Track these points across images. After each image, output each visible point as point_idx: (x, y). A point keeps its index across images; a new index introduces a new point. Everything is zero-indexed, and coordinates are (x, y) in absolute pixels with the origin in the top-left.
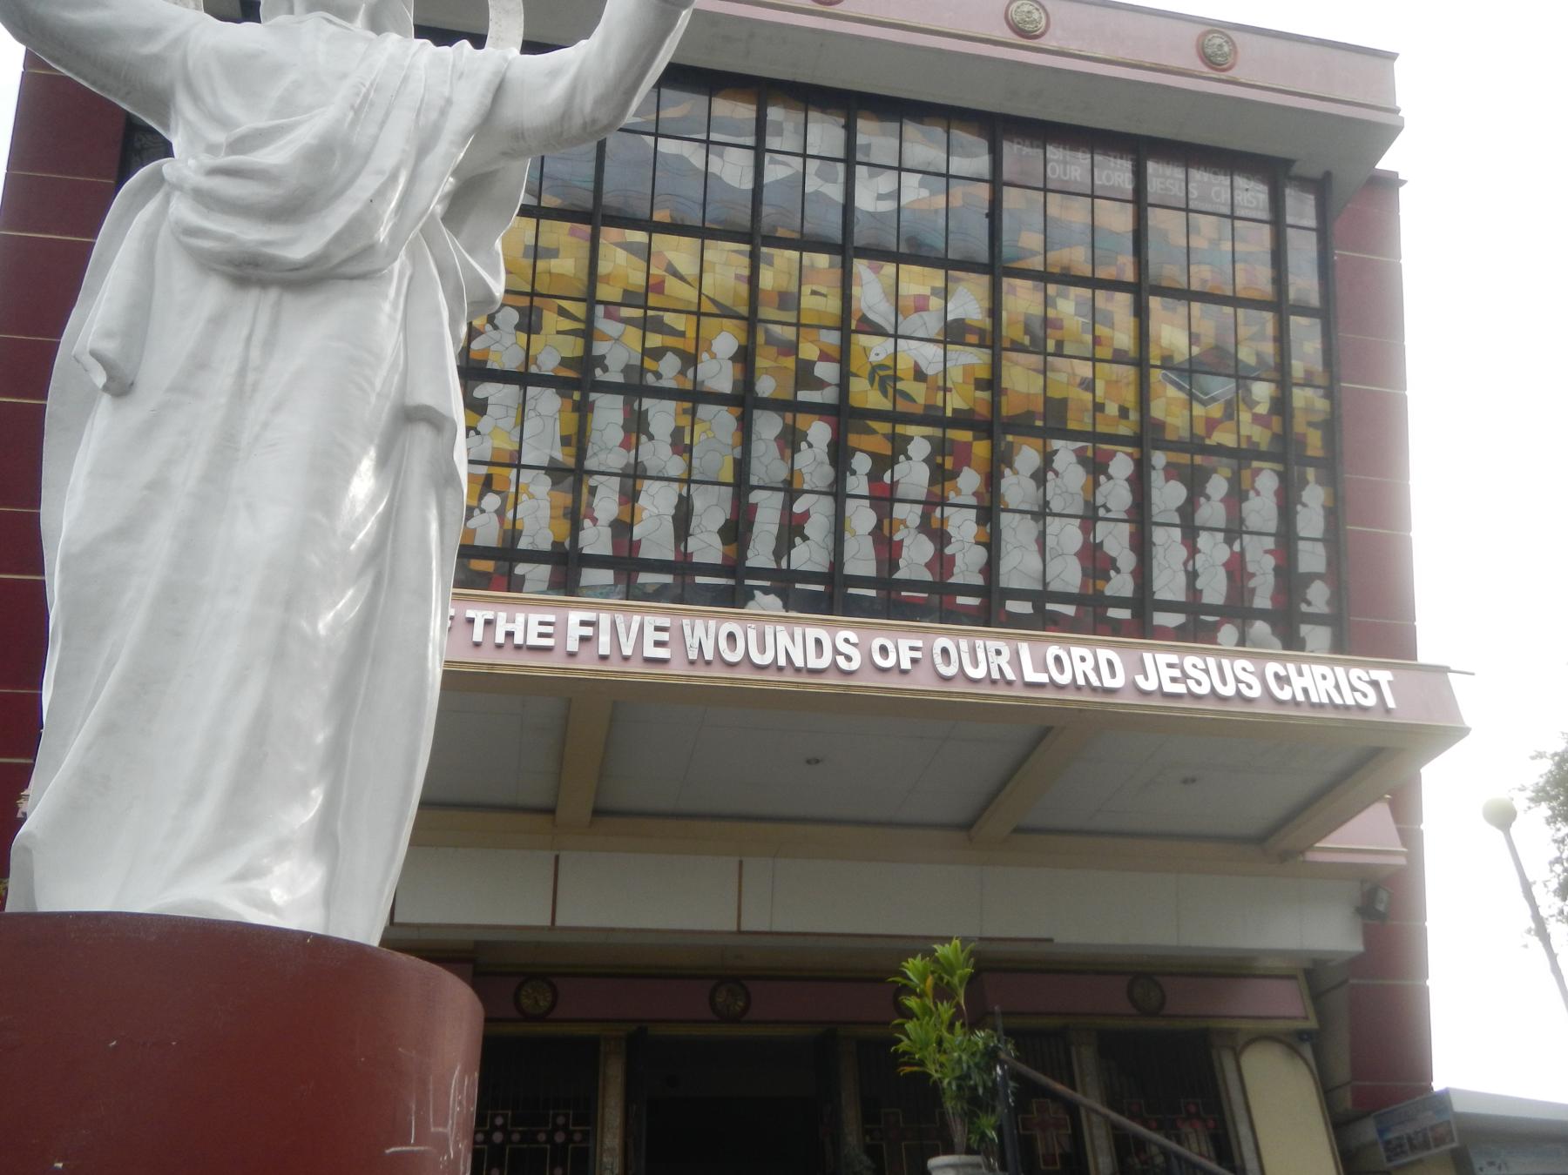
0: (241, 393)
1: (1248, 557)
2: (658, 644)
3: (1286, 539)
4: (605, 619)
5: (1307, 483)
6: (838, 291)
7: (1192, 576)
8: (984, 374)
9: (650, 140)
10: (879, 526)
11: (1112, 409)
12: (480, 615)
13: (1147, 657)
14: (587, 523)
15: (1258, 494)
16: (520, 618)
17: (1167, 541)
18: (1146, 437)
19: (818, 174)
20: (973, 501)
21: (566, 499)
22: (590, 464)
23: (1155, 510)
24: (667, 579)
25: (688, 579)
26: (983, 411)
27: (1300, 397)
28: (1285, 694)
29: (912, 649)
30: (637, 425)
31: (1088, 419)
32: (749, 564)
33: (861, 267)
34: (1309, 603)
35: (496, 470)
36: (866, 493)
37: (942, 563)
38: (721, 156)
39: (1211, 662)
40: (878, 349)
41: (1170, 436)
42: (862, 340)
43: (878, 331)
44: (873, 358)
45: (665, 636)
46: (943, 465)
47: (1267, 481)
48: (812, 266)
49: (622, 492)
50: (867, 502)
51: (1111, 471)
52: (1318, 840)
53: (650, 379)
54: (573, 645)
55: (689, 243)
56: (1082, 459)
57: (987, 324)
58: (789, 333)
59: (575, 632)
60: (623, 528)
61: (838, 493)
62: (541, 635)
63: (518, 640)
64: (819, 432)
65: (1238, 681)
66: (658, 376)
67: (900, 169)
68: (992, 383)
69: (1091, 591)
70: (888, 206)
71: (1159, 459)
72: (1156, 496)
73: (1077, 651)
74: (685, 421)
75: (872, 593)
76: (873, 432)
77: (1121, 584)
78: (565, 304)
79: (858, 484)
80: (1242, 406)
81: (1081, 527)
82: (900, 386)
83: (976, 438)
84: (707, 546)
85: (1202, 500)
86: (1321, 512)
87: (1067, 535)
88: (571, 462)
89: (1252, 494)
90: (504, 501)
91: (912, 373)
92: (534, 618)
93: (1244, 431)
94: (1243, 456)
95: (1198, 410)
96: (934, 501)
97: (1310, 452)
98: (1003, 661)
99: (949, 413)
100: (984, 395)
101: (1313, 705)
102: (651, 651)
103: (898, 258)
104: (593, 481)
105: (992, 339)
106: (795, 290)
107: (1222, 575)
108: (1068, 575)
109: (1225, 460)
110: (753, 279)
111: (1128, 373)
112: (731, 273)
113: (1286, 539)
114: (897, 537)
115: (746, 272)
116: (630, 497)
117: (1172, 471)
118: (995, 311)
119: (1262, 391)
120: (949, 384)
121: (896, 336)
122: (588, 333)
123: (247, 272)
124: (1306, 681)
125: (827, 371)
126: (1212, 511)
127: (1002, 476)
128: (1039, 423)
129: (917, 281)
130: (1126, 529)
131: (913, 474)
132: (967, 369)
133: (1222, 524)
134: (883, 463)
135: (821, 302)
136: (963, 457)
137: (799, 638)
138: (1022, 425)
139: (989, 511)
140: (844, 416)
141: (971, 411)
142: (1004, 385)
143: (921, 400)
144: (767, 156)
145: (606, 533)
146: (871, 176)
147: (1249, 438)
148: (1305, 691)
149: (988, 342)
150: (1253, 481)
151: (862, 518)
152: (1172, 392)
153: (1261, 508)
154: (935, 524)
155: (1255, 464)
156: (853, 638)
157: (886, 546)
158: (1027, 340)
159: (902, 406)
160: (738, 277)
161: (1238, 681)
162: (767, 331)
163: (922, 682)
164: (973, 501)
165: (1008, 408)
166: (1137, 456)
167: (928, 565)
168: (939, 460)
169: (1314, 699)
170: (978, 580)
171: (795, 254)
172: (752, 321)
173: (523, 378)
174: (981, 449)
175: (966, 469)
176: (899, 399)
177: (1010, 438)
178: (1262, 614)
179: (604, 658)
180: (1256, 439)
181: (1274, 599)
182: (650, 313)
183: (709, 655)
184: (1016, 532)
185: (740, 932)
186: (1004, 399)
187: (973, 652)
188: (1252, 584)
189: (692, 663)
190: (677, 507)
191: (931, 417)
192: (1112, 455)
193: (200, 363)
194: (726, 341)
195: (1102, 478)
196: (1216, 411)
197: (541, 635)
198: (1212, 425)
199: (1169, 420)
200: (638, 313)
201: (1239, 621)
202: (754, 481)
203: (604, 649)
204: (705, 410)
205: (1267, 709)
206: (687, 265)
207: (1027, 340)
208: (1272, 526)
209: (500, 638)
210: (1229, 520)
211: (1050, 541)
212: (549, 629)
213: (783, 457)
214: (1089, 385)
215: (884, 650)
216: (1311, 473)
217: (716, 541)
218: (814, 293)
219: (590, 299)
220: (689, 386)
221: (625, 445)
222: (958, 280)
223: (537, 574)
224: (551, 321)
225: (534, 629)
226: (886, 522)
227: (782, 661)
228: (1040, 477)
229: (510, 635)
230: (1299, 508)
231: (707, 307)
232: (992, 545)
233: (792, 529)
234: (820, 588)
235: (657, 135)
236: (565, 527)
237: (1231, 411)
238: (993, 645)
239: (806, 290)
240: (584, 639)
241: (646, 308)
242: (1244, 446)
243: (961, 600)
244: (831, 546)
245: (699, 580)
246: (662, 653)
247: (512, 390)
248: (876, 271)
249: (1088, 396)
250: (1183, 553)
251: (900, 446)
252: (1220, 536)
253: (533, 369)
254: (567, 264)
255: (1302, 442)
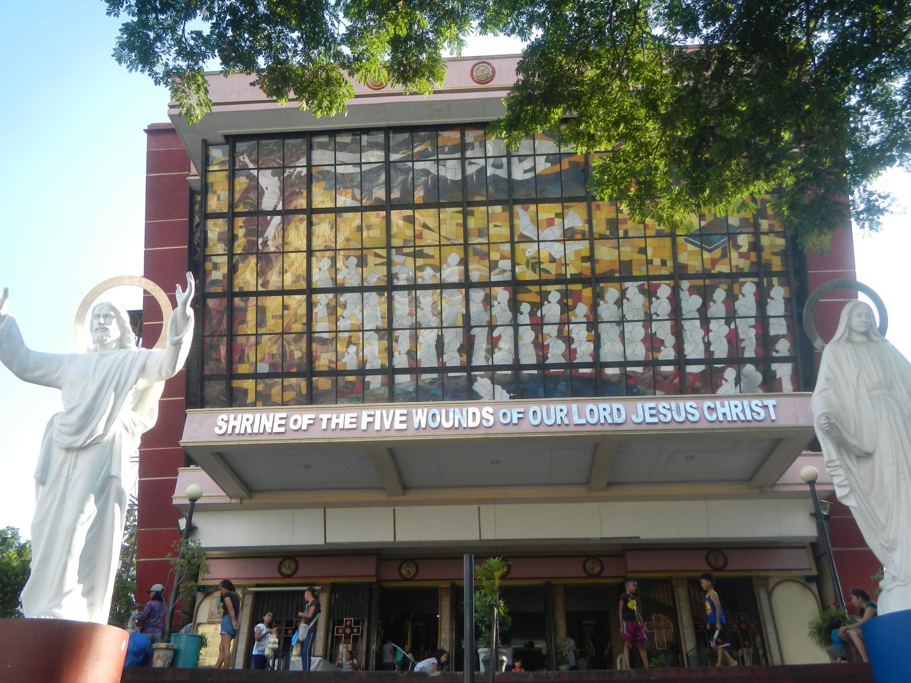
0: (67, 482)
1: (740, 331)
2: (401, 422)
3: (762, 320)
4: (378, 413)
5: (773, 286)
6: (508, 224)
7: (707, 345)
8: (586, 253)
9: (410, 164)
10: (537, 337)
11: (657, 262)
12: (325, 417)
13: (639, 405)
14: (396, 354)
15: (744, 296)
16: (342, 416)
17: (693, 330)
18: (679, 273)
19: (494, 166)
20: (585, 320)
21: (385, 343)
22: (395, 325)
23: (684, 312)
24: (435, 376)
25: (445, 375)
26: (588, 273)
27: (765, 240)
28: (714, 418)
29: (518, 413)
30: (416, 303)
31: (644, 269)
32: (473, 364)
33: (518, 209)
34: (777, 352)
35: (352, 334)
36: (529, 322)
37: (571, 353)
38: (444, 166)
39: (673, 405)
40: (530, 250)
41: (691, 271)
42: (520, 247)
43: (529, 240)
44: (527, 254)
45: (404, 418)
46: (566, 304)
47: (749, 288)
48: (494, 213)
49: (411, 338)
50: (529, 327)
51: (658, 295)
52: (778, 479)
53: (420, 281)
54: (364, 427)
55: (433, 211)
56: (641, 290)
57: (586, 228)
58: (485, 248)
59: (365, 419)
60: (412, 354)
61: (515, 325)
62: (351, 423)
63: (341, 426)
64: (502, 295)
65: (687, 412)
66: (424, 280)
67: (535, 155)
68: (590, 258)
69: (651, 359)
70: (530, 175)
71: (685, 284)
72: (684, 304)
73: (602, 406)
74: (437, 298)
75: (535, 372)
76: (530, 291)
77: (667, 353)
78: (378, 251)
79: (524, 319)
80: (732, 249)
81: (644, 326)
82: (542, 266)
83: (583, 288)
84: (453, 358)
85: (711, 303)
86: (783, 301)
87: (636, 331)
88: (386, 326)
89: (740, 296)
90: (358, 349)
91: (548, 259)
92: (348, 415)
93: (734, 263)
94: (735, 276)
95: (706, 255)
96: (564, 322)
97: (774, 269)
98: (563, 414)
99: (569, 277)
100: (588, 264)
101: (729, 422)
102: (398, 426)
103: (537, 201)
104: (397, 333)
105: (590, 237)
106: (485, 225)
107: (725, 341)
108: (638, 351)
109: (723, 280)
110: (465, 224)
111: (668, 241)
112: (454, 222)
113: (762, 320)
114: (545, 343)
115: (461, 221)
116: (415, 339)
117: (692, 290)
118: (589, 221)
119: (744, 240)
120: (568, 262)
121: (539, 241)
122: (389, 264)
123: (68, 449)
124: (726, 410)
125: (506, 264)
126: (717, 308)
127: (598, 305)
128: (617, 275)
129: (547, 211)
130: (668, 324)
131: (552, 310)
132: (577, 252)
133: (723, 314)
134: (536, 306)
135: (500, 231)
136: (578, 297)
137: (465, 412)
138: (608, 278)
139: (593, 323)
140: (515, 285)
141: (580, 273)
142: (597, 256)
143: (553, 272)
144: (467, 162)
145: (405, 357)
146: (520, 161)
147: (737, 266)
148: (724, 414)
149: (587, 237)
150: (741, 289)
151: (527, 335)
152: (690, 247)
153: (747, 303)
154: (565, 334)
155: (741, 280)
156: (491, 410)
157: (540, 347)
158: (608, 233)
159: (545, 276)
160: (457, 225)
161: (687, 412)
162: (474, 250)
163: (525, 429)
164: (585, 320)
165: (600, 269)
166: (672, 284)
167: (563, 355)
168: (565, 301)
169: (729, 418)
170: (590, 360)
171: (484, 208)
172: (466, 245)
173: (361, 289)
174: (587, 292)
175: (579, 304)
176: (542, 273)
177: (602, 285)
178: (750, 361)
179: (378, 431)
180: (741, 266)
181: (756, 351)
182: (417, 249)
183: (423, 425)
184: (609, 333)
185: (481, 540)
186: (597, 266)
187: (548, 411)
188: (743, 345)
189: (417, 429)
190: (437, 341)
191: (560, 280)
192: (659, 285)
193: (59, 475)
194: (454, 257)
195: (654, 299)
196: (718, 253)
197: (351, 423)
198: (714, 262)
199: (690, 263)
200: (412, 250)
201: (736, 366)
202: (473, 324)
203: (377, 426)
204: (447, 293)
205: (703, 425)
206: (432, 223)
207: (608, 233)
208: (753, 313)
209: (333, 427)
210: (727, 312)
211: (627, 335)
212: (354, 420)
213: (486, 310)
214: (643, 251)
215: (505, 414)
216: (775, 281)
217: (457, 355)
218: (495, 226)
219: (389, 247)
220: (438, 282)
221: (410, 314)
222: (569, 207)
223: (375, 382)
224: (371, 260)
225: (348, 420)
226: (540, 336)
227: (457, 425)
228: (619, 303)
229: (337, 424)
230: (769, 300)
231: (444, 242)
232: (597, 342)
233: (493, 343)
234: (510, 372)
235: (413, 161)
236: (386, 355)
237: (725, 255)
238: (559, 407)
239: (491, 225)
240: (368, 423)
241: (415, 246)
242: (734, 270)
243: (581, 371)
244: (513, 350)
245: (450, 375)
246: (404, 426)
247: (358, 295)
248: (526, 209)
249: (644, 257)
250: (702, 332)
251: (544, 296)
252: (723, 321)
253: (365, 284)
254: (375, 234)
255: (769, 264)
